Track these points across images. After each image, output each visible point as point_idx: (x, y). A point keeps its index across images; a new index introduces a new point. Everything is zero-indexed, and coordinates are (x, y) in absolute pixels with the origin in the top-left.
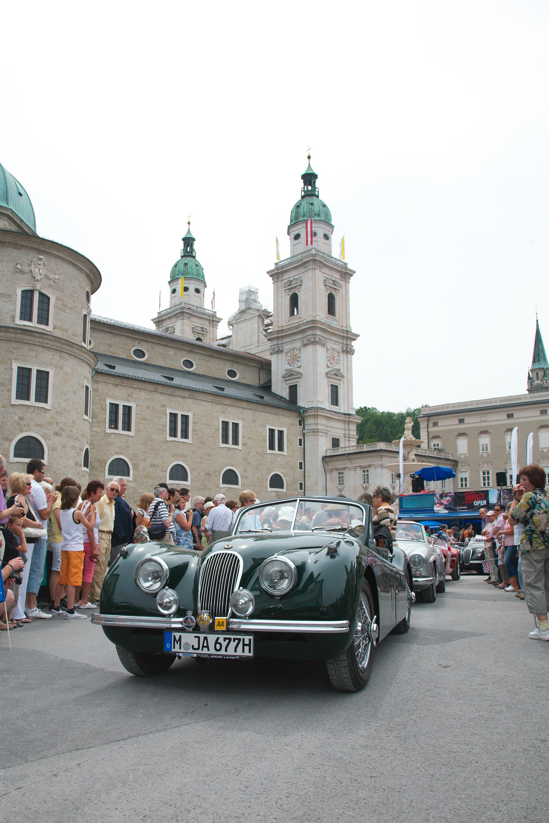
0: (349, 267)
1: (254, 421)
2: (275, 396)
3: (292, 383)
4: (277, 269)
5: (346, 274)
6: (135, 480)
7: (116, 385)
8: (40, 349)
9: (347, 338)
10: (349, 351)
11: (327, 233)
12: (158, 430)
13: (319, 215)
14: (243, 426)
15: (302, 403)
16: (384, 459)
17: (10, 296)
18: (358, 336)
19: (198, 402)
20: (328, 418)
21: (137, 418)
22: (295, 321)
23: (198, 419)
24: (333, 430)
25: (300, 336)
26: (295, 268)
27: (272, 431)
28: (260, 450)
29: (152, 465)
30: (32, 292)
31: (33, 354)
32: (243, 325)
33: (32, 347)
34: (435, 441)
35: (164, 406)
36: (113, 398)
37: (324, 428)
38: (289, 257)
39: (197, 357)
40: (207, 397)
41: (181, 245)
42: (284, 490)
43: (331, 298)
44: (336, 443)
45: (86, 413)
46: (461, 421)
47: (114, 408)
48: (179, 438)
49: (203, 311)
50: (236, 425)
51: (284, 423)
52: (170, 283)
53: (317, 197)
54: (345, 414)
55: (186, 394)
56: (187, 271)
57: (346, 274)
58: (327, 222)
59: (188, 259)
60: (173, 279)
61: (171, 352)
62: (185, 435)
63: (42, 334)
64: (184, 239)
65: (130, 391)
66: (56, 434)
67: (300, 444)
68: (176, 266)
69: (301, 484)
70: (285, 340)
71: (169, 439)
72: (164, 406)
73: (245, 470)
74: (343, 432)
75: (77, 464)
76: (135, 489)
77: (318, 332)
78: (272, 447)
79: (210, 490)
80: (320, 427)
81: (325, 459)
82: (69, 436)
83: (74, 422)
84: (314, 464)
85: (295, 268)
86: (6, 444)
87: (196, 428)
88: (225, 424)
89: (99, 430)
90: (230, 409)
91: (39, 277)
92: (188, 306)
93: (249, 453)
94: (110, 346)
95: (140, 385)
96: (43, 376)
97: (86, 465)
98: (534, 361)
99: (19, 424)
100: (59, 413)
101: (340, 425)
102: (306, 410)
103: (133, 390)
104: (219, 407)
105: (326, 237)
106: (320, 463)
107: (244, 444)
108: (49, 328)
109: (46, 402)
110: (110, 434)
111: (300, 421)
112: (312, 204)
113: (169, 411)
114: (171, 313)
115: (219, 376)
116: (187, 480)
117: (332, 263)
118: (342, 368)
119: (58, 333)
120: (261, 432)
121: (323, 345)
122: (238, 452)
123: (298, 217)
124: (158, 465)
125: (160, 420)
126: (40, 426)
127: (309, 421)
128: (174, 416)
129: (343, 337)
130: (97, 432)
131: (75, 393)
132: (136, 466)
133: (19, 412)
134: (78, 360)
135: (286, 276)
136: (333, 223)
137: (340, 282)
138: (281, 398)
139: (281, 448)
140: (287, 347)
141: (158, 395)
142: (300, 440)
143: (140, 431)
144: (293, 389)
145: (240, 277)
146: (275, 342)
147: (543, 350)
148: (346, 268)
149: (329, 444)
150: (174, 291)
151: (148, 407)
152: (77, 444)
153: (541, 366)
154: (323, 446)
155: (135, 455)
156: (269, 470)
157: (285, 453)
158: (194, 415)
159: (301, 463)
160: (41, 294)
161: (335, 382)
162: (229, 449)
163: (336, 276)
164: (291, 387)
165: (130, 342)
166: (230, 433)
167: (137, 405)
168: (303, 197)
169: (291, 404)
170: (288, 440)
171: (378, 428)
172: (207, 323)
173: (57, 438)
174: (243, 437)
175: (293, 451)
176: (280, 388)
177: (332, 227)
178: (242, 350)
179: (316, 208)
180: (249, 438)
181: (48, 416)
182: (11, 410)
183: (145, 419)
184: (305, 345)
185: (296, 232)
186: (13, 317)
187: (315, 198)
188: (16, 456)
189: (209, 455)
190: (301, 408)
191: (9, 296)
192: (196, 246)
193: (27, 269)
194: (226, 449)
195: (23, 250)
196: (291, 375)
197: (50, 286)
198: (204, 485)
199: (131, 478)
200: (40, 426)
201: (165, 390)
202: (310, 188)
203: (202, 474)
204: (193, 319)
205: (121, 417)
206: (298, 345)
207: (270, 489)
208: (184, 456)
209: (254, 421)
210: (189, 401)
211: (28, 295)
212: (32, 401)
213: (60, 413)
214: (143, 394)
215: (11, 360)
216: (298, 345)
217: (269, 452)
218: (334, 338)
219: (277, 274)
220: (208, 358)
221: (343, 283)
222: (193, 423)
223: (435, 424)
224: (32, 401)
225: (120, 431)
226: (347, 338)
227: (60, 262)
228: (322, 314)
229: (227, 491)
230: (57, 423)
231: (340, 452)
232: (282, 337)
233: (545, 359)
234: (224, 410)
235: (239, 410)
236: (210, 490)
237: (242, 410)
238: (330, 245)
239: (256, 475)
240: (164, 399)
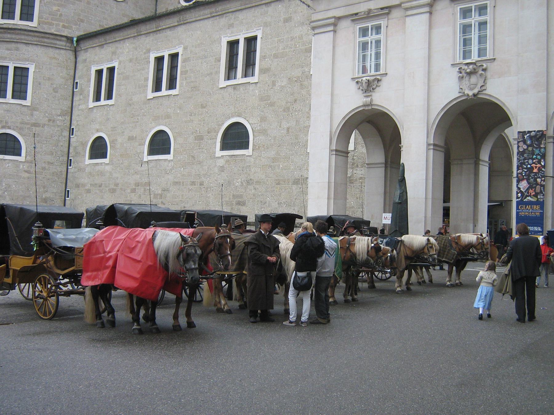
1: (287, 20)
7: (101, 46)
12: (139, 88)
19: (193, 25)
23: (191, 52)
28: (297, 73)
29: (131, 138)
40: (202, 13)
72: (149, 51)
73: (263, 119)
76: (111, 173)
79: (200, 163)
87: (188, 69)
89: (82, 107)
90: (241, 16)
93: (274, 84)
95: (119, 35)
103: (117, 45)
104: (223, 21)
107: (261, 71)
116: (169, 153)
120: (301, 37)
122: (251, 88)
124: (136, 137)
125: (143, 72)
130: (82, 110)
141: (143, 38)
143: (120, 95)
151: (131, 61)
155: (114, 129)
158: (185, 48)
162: (235, 86)
167: (120, 63)
174: (263, 58)
180: (276, 56)
189: (203, 107)
194: (230, 90)
198: (193, 157)
208: (168, 117)
209: (287, 20)
210: (181, 29)
222: (184, 61)
229: (227, 161)
234: (232, 21)
236: (200, 163)
237: (264, 8)
239: (285, 125)
240: (146, 41)
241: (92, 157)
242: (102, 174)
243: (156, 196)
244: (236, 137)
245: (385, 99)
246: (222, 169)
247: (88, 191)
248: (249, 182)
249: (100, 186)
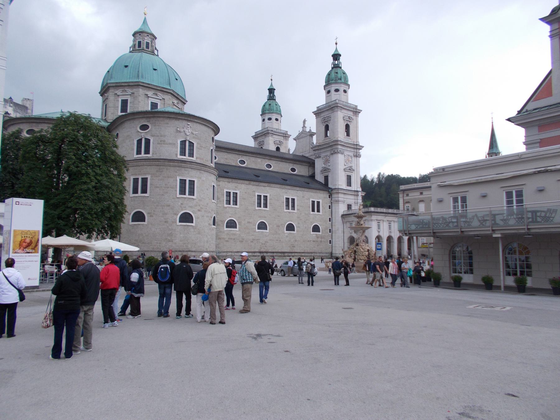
0: (359, 108)
1: (303, 197)
2: (317, 181)
3: (326, 174)
4: (318, 110)
5: (356, 112)
6: (239, 230)
7: (229, 182)
8: (190, 170)
9: (357, 149)
10: (358, 156)
11: (345, 89)
13: (341, 79)
14: (297, 200)
15: (330, 186)
16: (373, 216)
17: (174, 144)
18: (363, 147)
20: (345, 194)
21: (240, 198)
22: (327, 140)
24: (348, 200)
25: (330, 149)
26: (327, 110)
27: (313, 202)
28: (307, 212)
30: (185, 141)
31: (187, 172)
32: (301, 140)
33: (186, 169)
34: (407, 205)
35: (254, 192)
36: (228, 189)
37: (342, 199)
38: (325, 103)
39: (274, 162)
41: (267, 93)
42: (320, 233)
43: (347, 127)
44: (349, 207)
45: (214, 199)
46: (421, 193)
47: (228, 194)
48: (262, 208)
49: (280, 131)
50: (293, 200)
51: (321, 197)
52: (261, 115)
53: (341, 68)
54: (355, 191)
55: (266, 185)
56: (270, 107)
57: (356, 112)
58: (346, 83)
59: (271, 101)
60: (263, 114)
61: (259, 160)
62: (266, 206)
63: (191, 162)
64: (269, 89)
65: (236, 185)
66: (199, 210)
67: (330, 208)
68: (264, 105)
69: (330, 230)
70: (322, 151)
71: (257, 208)
72: (254, 192)
73: (299, 223)
74: (354, 201)
77: (339, 147)
78: (313, 210)
80: (340, 199)
81: (343, 216)
83: (207, 204)
84: (338, 219)
85: (327, 110)
86: (175, 216)
88: (287, 199)
90: (290, 191)
91: (188, 134)
92: (271, 129)
94: (226, 159)
96: (192, 183)
97: (214, 224)
98: (490, 148)
99: (181, 207)
101: (353, 197)
102: (332, 190)
104: (284, 190)
105: (345, 91)
106: (340, 219)
107: (298, 210)
108: (194, 159)
109: (194, 195)
110: (226, 207)
111: (329, 196)
112: (337, 73)
113: (257, 194)
114: (262, 133)
115: (286, 171)
117: (348, 107)
118: (353, 165)
119: (198, 161)
121: (342, 154)
123: (329, 81)
126: (191, 207)
127: (334, 196)
128: (259, 196)
129: (354, 148)
132: (240, 223)
133: (181, 201)
134: (208, 174)
135: (322, 115)
136: (349, 83)
137: (353, 117)
138: (320, 183)
139: (318, 211)
140: (323, 155)
141: (251, 186)
142: (330, 206)
144: (326, 178)
145: (300, 112)
146: (317, 152)
147: (495, 141)
148: (356, 109)
149: (346, 209)
150: (264, 120)
152: (209, 215)
153: (494, 151)
154: (342, 209)
156: (312, 223)
157: (321, 213)
159: (330, 219)
160: (190, 142)
161: (349, 174)
162: (289, 212)
163: (350, 114)
164: (325, 177)
165: (237, 156)
166: (290, 203)
168: (332, 68)
169: (325, 187)
170: (322, 206)
171: (383, 194)
172: (282, 138)
174: (297, 206)
175: (325, 212)
176: (320, 178)
177: (349, 86)
178: (301, 154)
179: (339, 76)
182: (177, 200)
183: (244, 199)
184: (332, 154)
185: (328, 89)
186: (177, 155)
187: (339, 69)
188: (180, 222)
190: (330, 188)
191: (174, 144)
192: (276, 93)
193: (182, 130)
195: (180, 121)
196: (325, 170)
197: (194, 138)
199: (237, 229)
200: (191, 207)
201: (255, 183)
202: (336, 62)
203: (275, 226)
204: (274, 136)
205: (232, 199)
206: (328, 153)
207: (312, 233)
208: (265, 217)
209: (303, 197)
210: (268, 188)
211: (183, 143)
212: (187, 195)
214: (243, 186)
215: (176, 176)
216: (328, 153)
217: (312, 213)
218: (349, 149)
219: (318, 113)
220: (279, 162)
221: (354, 117)
222: (270, 199)
223: (407, 195)
224: (187, 195)
225: (232, 205)
226: (357, 148)
227: (198, 125)
228: (341, 135)
231: (350, 212)
232: (320, 149)
233: (496, 146)
235: (295, 191)
238: (347, 96)
241: (227, 227)
242: (234, 234)
243: (262, 244)
244: (290, 227)
245: (381, 234)
246: (287, 236)
247: (227, 241)
248: (296, 241)
249: (234, 239)
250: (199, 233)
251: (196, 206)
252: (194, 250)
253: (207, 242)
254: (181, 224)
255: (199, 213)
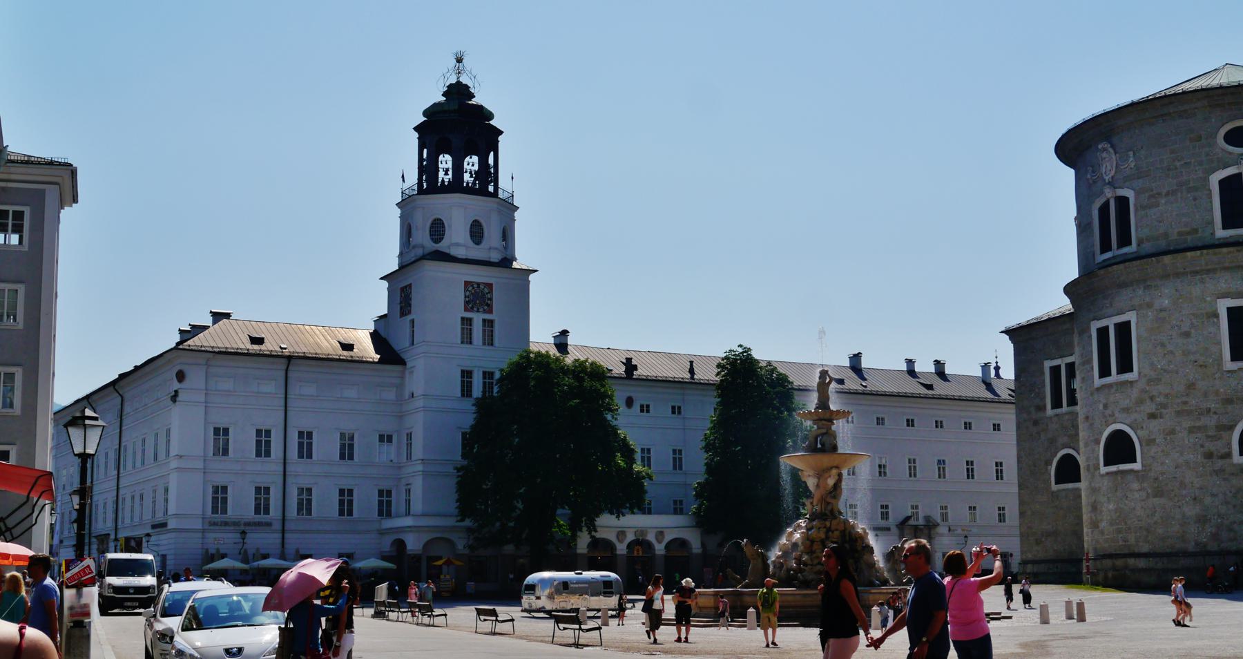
66: (1152, 416)
75: (1209, 456)
82: (1179, 413)
100: (1149, 381)
119: (1148, 247)
126: (1126, 410)
131: (1187, 335)
173: (1154, 423)
181: (1135, 393)
200: (1126, 410)
213: (1157, 380)
230: (1152, 398)
250: (1159, 493)
251: (1140, 402)
252: (1145, 548)
253: (1202, 520)
254: (1113, 468)
255: (1154, 425)
